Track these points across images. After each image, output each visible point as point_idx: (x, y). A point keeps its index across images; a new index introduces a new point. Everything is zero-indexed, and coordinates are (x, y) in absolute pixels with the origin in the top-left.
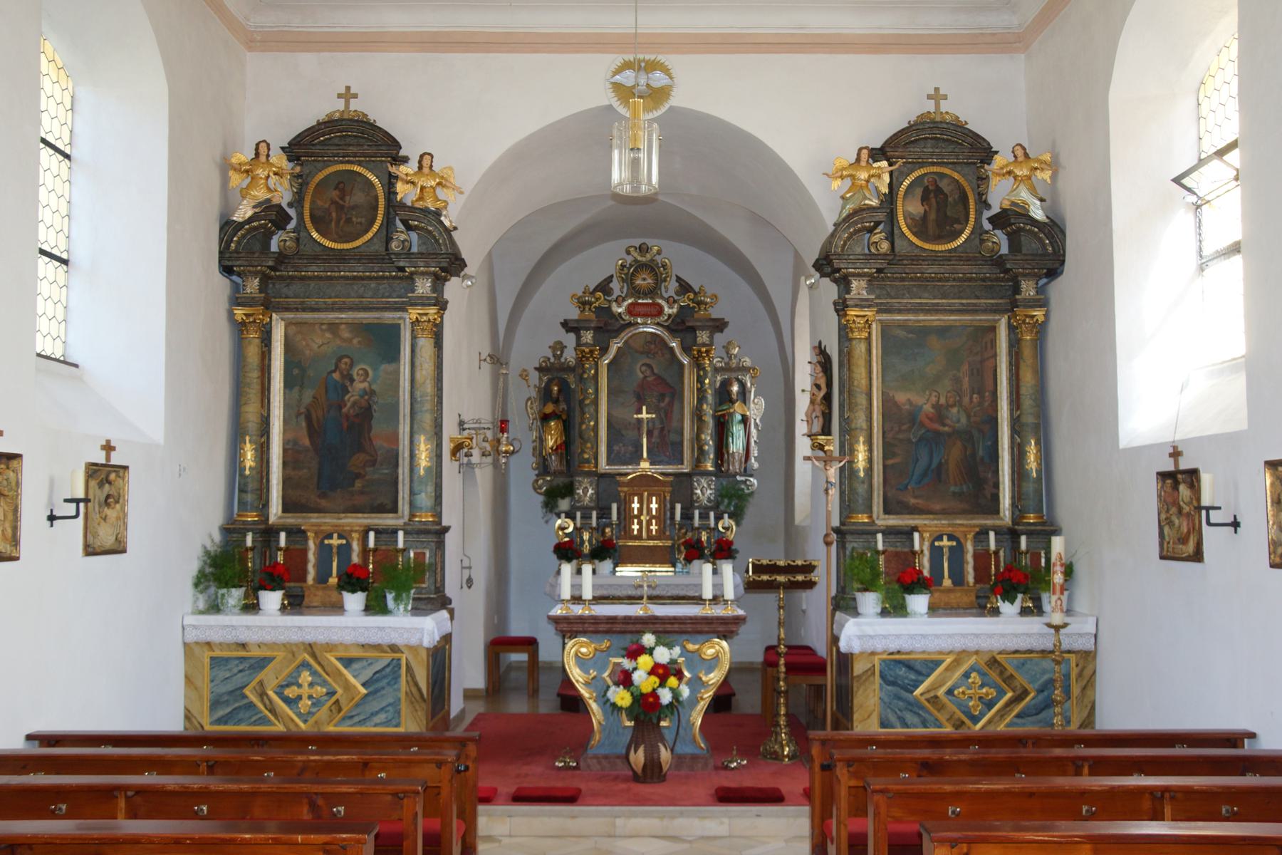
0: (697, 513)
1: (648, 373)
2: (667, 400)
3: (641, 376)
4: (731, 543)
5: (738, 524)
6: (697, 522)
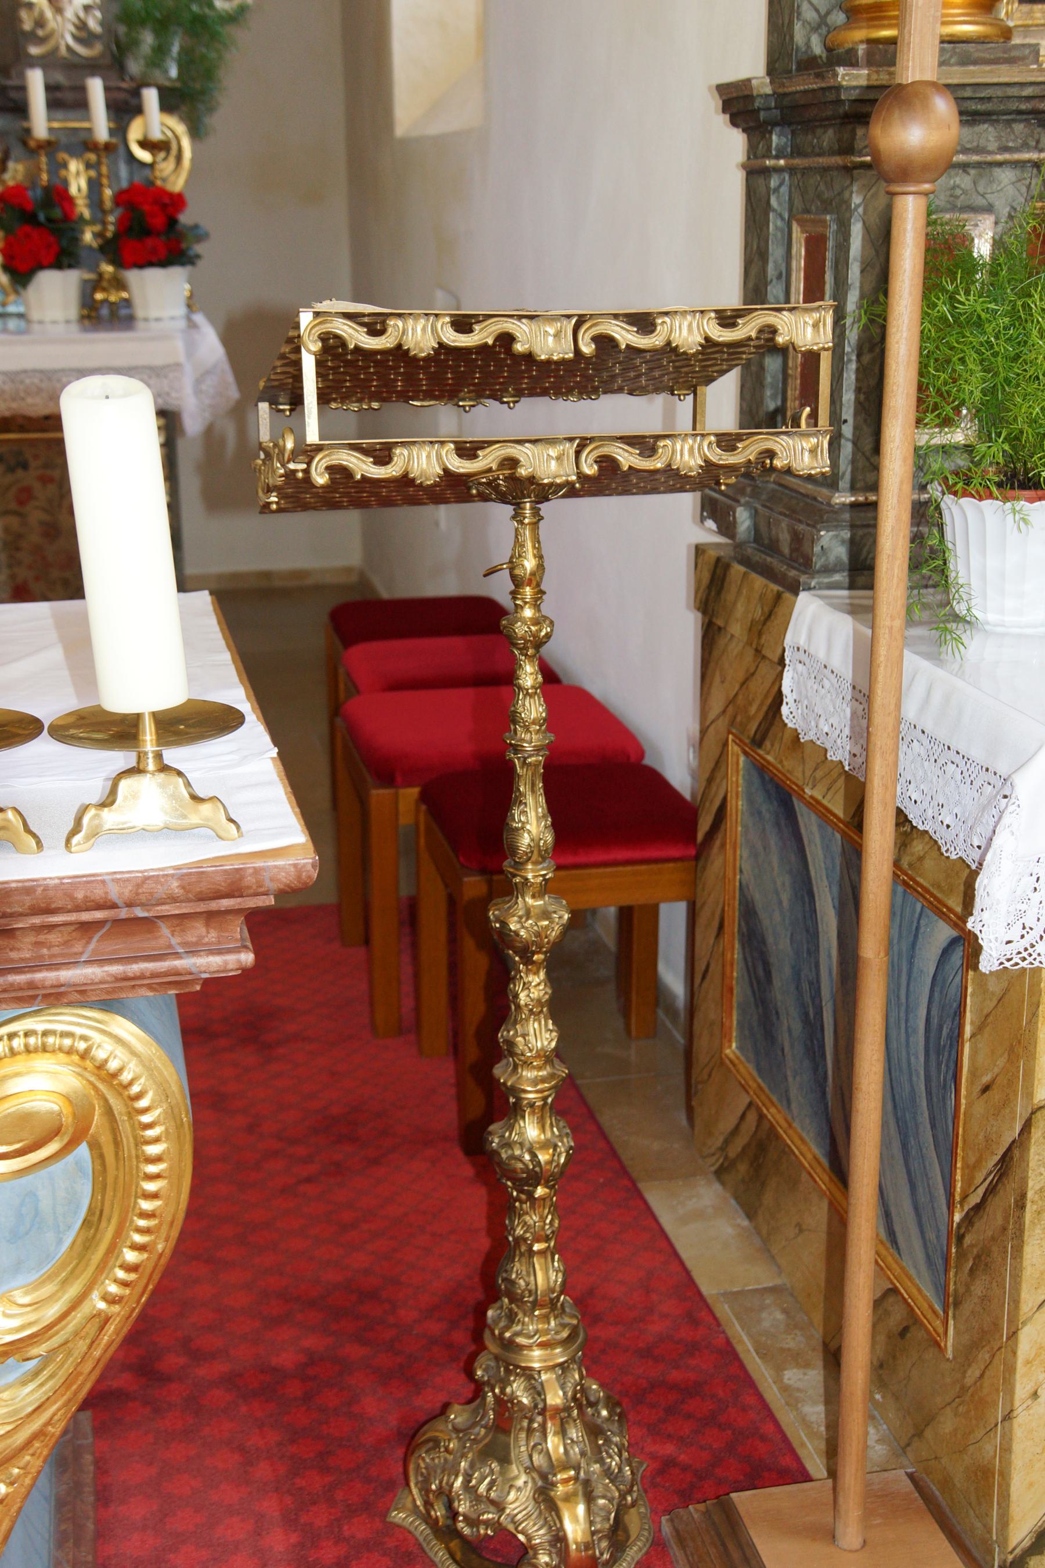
0: (36, 81)
4: (177, 202)
5: (196, 132)
6: (40, 121)
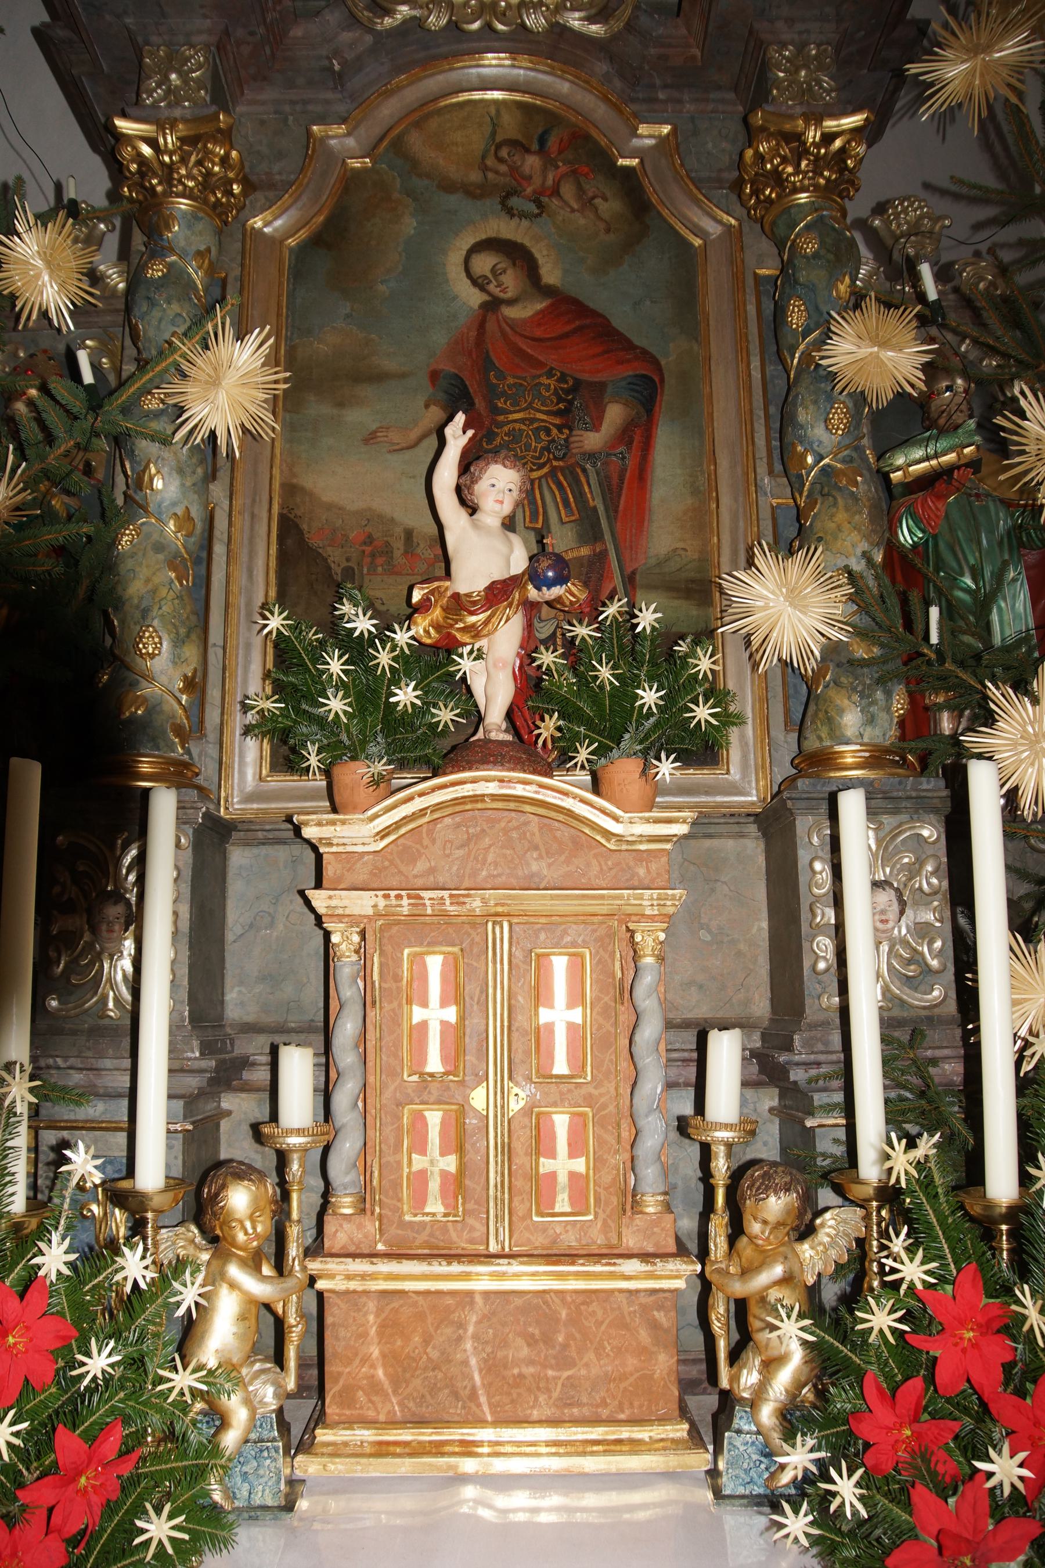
1: (511, 282)
2: (614, 414)
3: (474, 298)
